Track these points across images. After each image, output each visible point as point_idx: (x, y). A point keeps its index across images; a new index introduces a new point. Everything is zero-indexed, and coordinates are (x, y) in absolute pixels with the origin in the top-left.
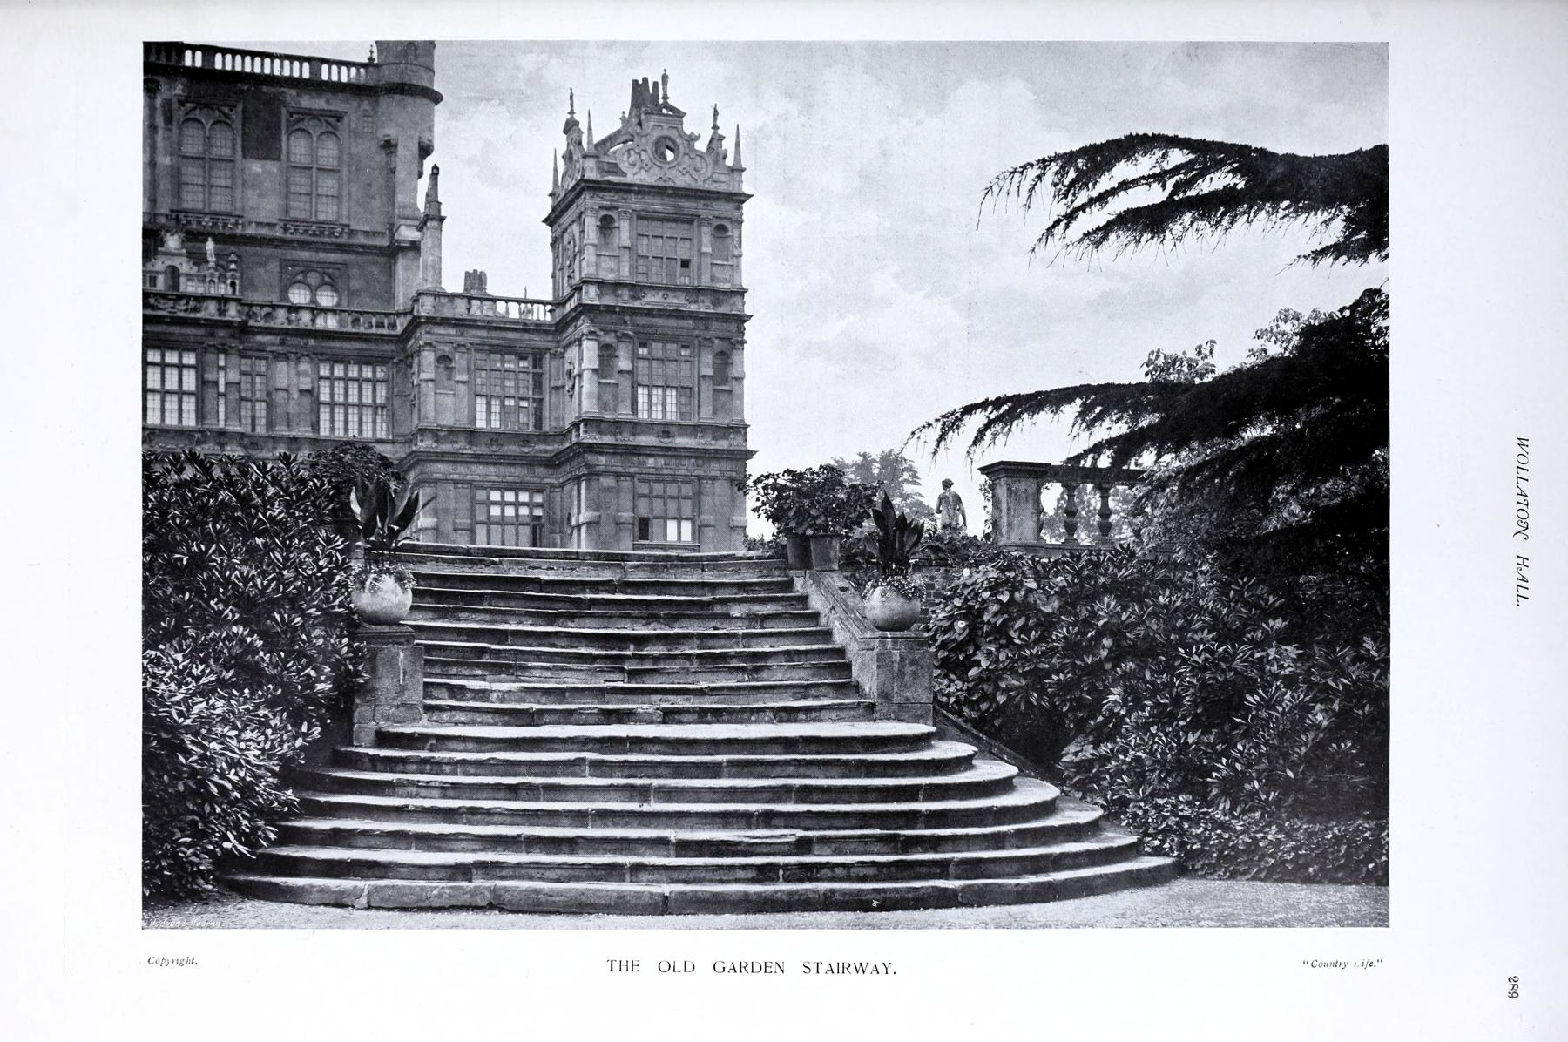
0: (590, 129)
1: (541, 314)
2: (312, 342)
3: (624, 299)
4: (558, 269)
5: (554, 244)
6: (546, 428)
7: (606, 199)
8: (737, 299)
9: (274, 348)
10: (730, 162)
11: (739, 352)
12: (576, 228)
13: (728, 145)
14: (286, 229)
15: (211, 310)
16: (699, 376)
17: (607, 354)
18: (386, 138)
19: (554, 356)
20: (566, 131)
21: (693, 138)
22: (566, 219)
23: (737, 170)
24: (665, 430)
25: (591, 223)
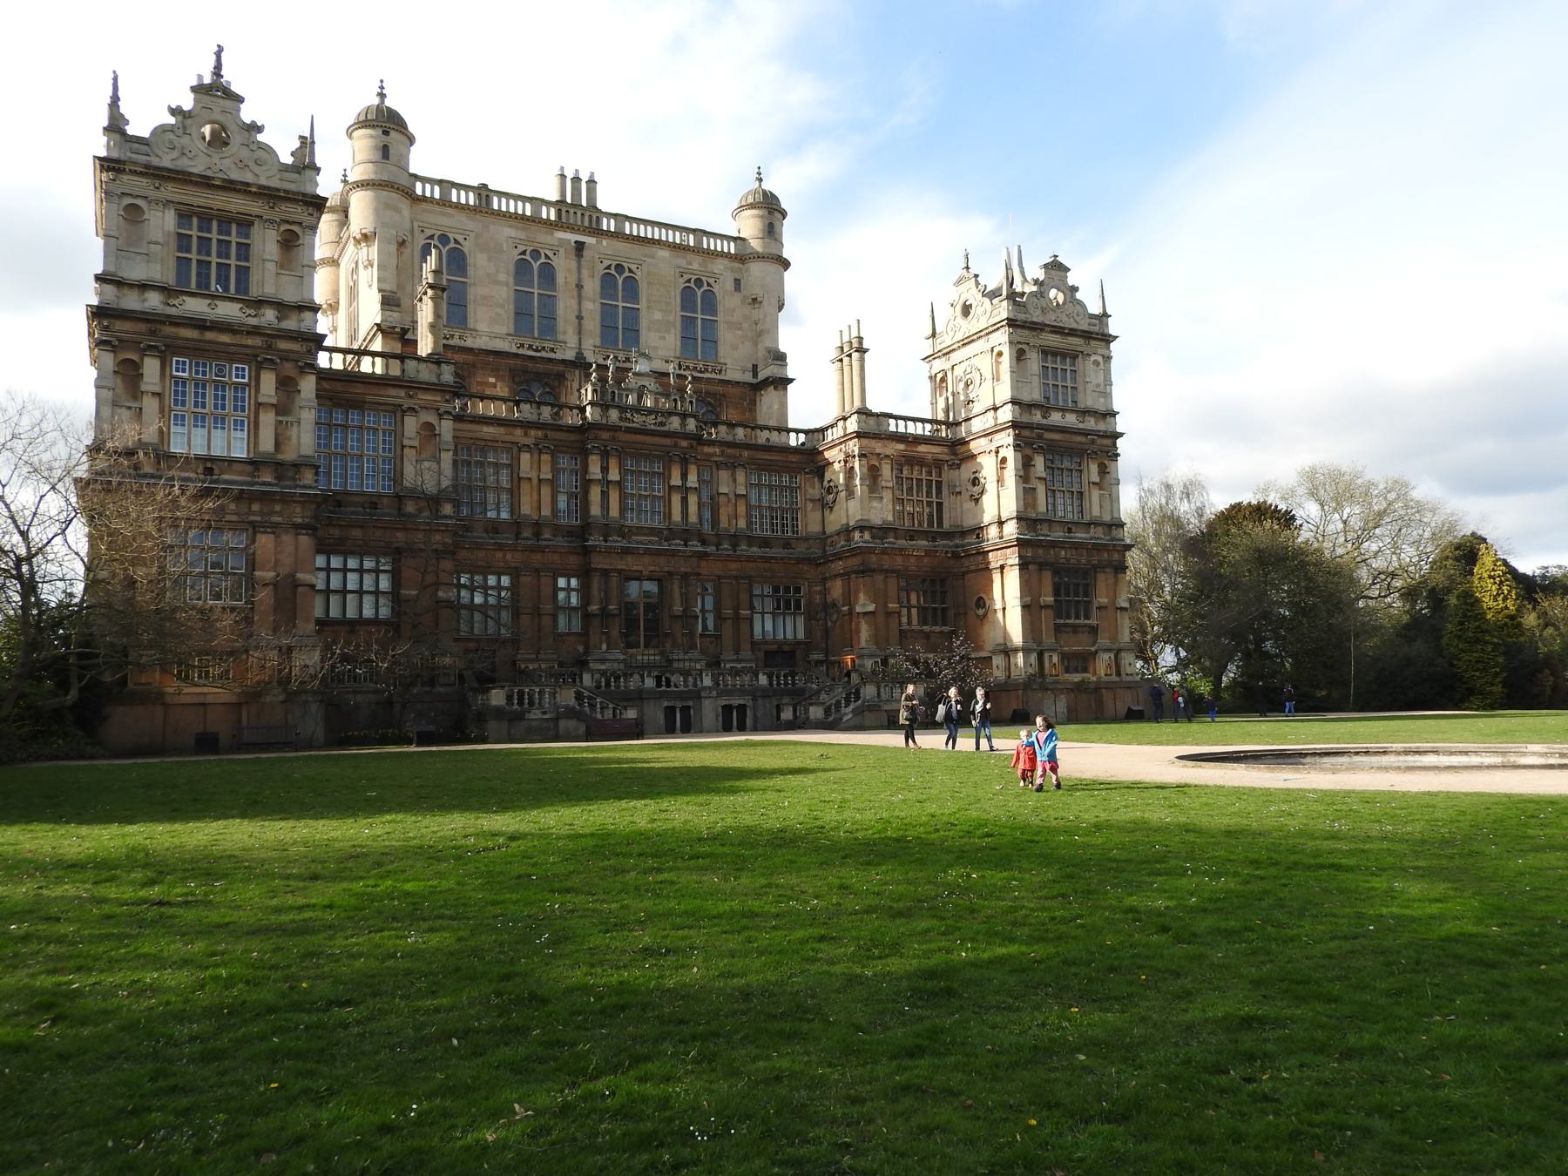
2: (746, 454)
3: (1037, 417)
6: (946, 525)
9: (716, 459)
11: (1114, 463)
14: (680, 369)
15: (675, 423)
19: (951, 467)
24: (1069, 526)
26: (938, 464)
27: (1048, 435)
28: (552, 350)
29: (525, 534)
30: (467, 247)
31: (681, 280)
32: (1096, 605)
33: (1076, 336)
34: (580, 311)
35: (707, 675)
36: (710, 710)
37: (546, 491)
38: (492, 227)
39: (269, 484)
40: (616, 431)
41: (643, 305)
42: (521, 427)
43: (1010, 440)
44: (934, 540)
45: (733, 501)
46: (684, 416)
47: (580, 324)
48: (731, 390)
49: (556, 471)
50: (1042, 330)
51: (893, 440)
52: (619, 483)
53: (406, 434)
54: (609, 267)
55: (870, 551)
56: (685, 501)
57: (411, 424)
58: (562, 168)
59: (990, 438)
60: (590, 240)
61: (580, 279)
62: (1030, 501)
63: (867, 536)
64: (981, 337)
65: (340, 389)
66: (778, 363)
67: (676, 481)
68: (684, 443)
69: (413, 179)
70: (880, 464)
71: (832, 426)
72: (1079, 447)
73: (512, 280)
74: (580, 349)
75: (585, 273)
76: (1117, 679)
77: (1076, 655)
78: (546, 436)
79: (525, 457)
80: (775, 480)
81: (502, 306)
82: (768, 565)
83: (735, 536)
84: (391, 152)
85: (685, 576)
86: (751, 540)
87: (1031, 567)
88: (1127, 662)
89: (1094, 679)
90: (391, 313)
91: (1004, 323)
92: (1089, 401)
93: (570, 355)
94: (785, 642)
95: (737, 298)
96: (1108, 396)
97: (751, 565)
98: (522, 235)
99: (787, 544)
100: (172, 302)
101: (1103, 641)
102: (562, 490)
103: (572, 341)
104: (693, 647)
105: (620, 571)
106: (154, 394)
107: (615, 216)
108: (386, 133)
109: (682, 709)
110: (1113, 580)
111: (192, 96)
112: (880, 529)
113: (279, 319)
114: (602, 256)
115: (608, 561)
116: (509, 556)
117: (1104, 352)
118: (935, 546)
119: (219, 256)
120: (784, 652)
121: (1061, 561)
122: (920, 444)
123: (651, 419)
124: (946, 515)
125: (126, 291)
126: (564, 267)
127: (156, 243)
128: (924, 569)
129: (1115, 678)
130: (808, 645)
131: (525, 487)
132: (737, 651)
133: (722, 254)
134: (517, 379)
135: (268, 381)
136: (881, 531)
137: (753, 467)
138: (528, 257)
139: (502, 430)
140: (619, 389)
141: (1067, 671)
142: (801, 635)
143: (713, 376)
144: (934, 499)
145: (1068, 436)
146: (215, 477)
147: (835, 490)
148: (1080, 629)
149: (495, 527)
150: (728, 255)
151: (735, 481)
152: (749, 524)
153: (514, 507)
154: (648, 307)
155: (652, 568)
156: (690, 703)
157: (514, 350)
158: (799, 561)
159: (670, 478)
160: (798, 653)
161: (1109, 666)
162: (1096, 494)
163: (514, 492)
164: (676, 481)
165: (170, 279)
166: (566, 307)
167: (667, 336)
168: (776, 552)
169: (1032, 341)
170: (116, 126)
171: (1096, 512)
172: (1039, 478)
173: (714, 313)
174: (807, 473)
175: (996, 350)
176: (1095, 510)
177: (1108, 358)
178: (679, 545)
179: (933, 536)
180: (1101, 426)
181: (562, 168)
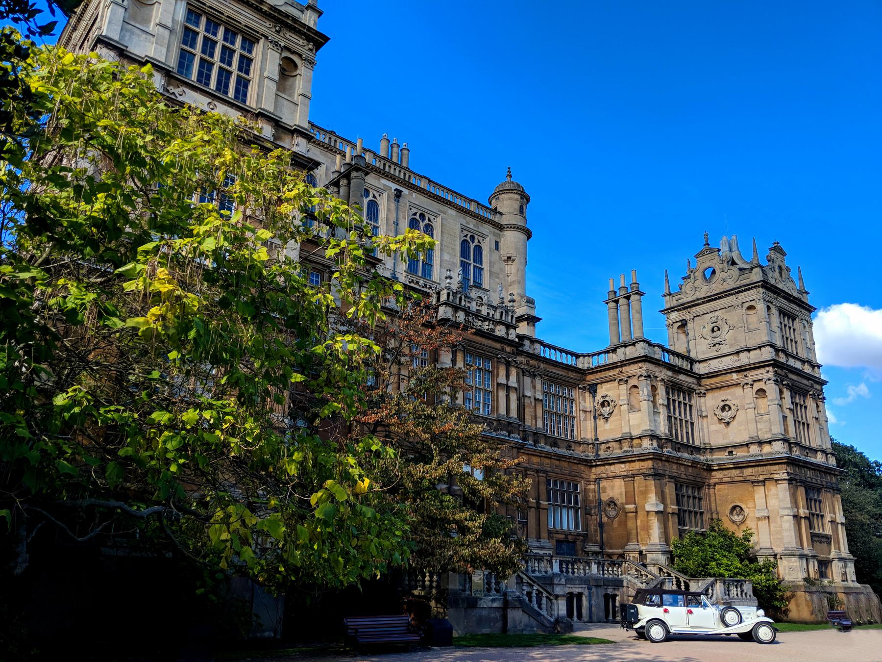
2: (542, 366)
9: (523, 367)
18: (508, 256)
27: (791, 376)
35: (556, 562)
43: (771, 375)
45: (533, 404)
50: (779, 295)
54: (415, 214)
59: (745, 373)
60: (405, 191)
66: (530, 305)
67: (502, 380)
68: (508, 349)
71: (588, 356)
74: (394, 271)
91: (760, 284)
97: (547, 461)
114: (412, 204)
124: (696, 434)
132: (539, 538)
147: (612, 404)
151: (534, 387)
152: (544, 425)
159: (498, 376)
175: (747, 305)
178: (506, 436)
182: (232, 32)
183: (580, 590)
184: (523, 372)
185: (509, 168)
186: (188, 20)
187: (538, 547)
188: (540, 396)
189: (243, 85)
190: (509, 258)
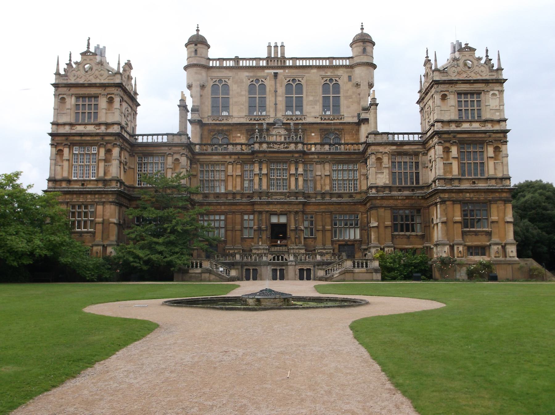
0: (436, 60)
1: (416, 138)
2: (329, 157)
3: (453, 127)
4: (423, 119)
5: (422, 109)
7: (442, 87)
8: (503, 124)
10: (495, 68)
12: (430, 102)
13: (495, 62)
14: (322, 119)
15: (292, 147)
16: (488, 158)
17: (447, 151)
20: (425, 65)
21: (480, 59)
22: (425, 100)
23: (500, 69)
25: (438, 97)
26: (416, 154)
27: (459, 136)
28: (264, 119)
29: (229, 198)
30: (230, 83)
31: (323, 81)
32: (490, 221)
33: (479, 83)
34: (276, 101)
36: (292, 271)
37: (239, 180)
38: (239, 73)
39: (101, 188)
40: (265, 153)
41: (304, 95)
42: (228, 155)
44: (413, 190)
45: (324, 178)
46: (296, 143)
47: (276, 107)
48: (347, 127)
49: (243, 171)
50: (456, 83)
51: (389, 145)
52: (267, 174)
53: (168, 163)
55: (375, 198)
56: (297, 180)
57: (170, 160)
58: (270, 43)
61: (276, 88)
62: (448, 169)
63: (374, 191)
64: (429, 90)
65: (145, 149)
67: (293, 171)
68: (296, 155)
69: (208, 61)
70: (383, 157)
72: (480, 139)
73: (247, 93)
75: (278, 85)
76: (503, 259)
77: (477, 247)
78: (239, 158)
79: (230, 167)
80: (345, 167)
81: (243, 105)
82: (339, 206)
83: (323, 193)
84: (198, 52)
85: (296, 213)
86: (332, 195)
87: (447, 203)
88: (510, 250)
89: (489, 259)
90: (194, 115)
92: (487, 115)
93: (271, 121)
94: (349, 240)
95: (350, 85)
96: (501, 111)
98: (251, 74)
99: (351, 196)
100: (73, 128)
101: (495, 239)
102: (246, 179)
103: (272, 114)
104: (300, 243)
105: (268, 211)
106: (67, 160)
107: (292, 59)
108: (196, 45)
109: (280, 270)
110: (503, 207)
111: (80, 56)
112: (382, 187)
113: (106, 129)
115: (262, 207)
116: (223, 207)
117: (500, 88)
118: (414, 194)
119: (88, 110)
120: (348, 245)
121: (467, 199)
122: (405, 145)
123: (282, 146)
125: (60, 127)
126: (269, 83)
127: (68, 109)
128: (406, 205)
129: (501, 258)
130: (360, 242)
131: (230, 179)
132: (324, 245)
133: (343, 66)
134: (249, 133)
135: (102, 151)
136: (384, 187)
137: (334, 162)
138: (254, 83)
139: (220, 157)
140: (267, 135)
141: (471, 254)
142: (358, 237)
143: (338, 121)
144: (414, 171)
145: (472, 135)
146: (85, 187)
148: (480, 233)
149: (218, 196)
150: (346, 67)
151: (324, 169)
152: (331, 188)
153: (226, 188)
154: (307, 95)
155: (281, 210)
156: (284, 268)
157: (248, 122)
158: (355, 204)
159: (290, 170)
160: (356, 245)
161: (497, 252)
162: (491, 163)
163: (226, 181)
164: (293, 171)
165: (73, 121)
166: (270, 101)
167: (315, 106)
168: (345, 199)
169: (451, 89)
170: (57, 74)
171: (491, 172)
172: (453, 158)
173: (339, 93)
174: (361, 163)
176: (491, 169)
177: (501, 92)
179: (413, 189)
180: (497, 127)
181: (270, 43)
182: (90, 97)
183: (308, 267)
184: (316, 163)
185: (362, 23)
186: (76, 101)
187: (321, 249)
188: (327, 173)
189: (96, 114)
190: (357, 84)
